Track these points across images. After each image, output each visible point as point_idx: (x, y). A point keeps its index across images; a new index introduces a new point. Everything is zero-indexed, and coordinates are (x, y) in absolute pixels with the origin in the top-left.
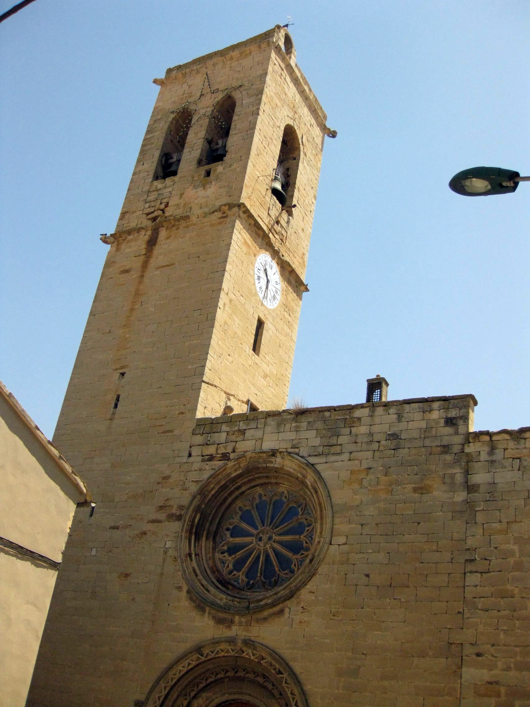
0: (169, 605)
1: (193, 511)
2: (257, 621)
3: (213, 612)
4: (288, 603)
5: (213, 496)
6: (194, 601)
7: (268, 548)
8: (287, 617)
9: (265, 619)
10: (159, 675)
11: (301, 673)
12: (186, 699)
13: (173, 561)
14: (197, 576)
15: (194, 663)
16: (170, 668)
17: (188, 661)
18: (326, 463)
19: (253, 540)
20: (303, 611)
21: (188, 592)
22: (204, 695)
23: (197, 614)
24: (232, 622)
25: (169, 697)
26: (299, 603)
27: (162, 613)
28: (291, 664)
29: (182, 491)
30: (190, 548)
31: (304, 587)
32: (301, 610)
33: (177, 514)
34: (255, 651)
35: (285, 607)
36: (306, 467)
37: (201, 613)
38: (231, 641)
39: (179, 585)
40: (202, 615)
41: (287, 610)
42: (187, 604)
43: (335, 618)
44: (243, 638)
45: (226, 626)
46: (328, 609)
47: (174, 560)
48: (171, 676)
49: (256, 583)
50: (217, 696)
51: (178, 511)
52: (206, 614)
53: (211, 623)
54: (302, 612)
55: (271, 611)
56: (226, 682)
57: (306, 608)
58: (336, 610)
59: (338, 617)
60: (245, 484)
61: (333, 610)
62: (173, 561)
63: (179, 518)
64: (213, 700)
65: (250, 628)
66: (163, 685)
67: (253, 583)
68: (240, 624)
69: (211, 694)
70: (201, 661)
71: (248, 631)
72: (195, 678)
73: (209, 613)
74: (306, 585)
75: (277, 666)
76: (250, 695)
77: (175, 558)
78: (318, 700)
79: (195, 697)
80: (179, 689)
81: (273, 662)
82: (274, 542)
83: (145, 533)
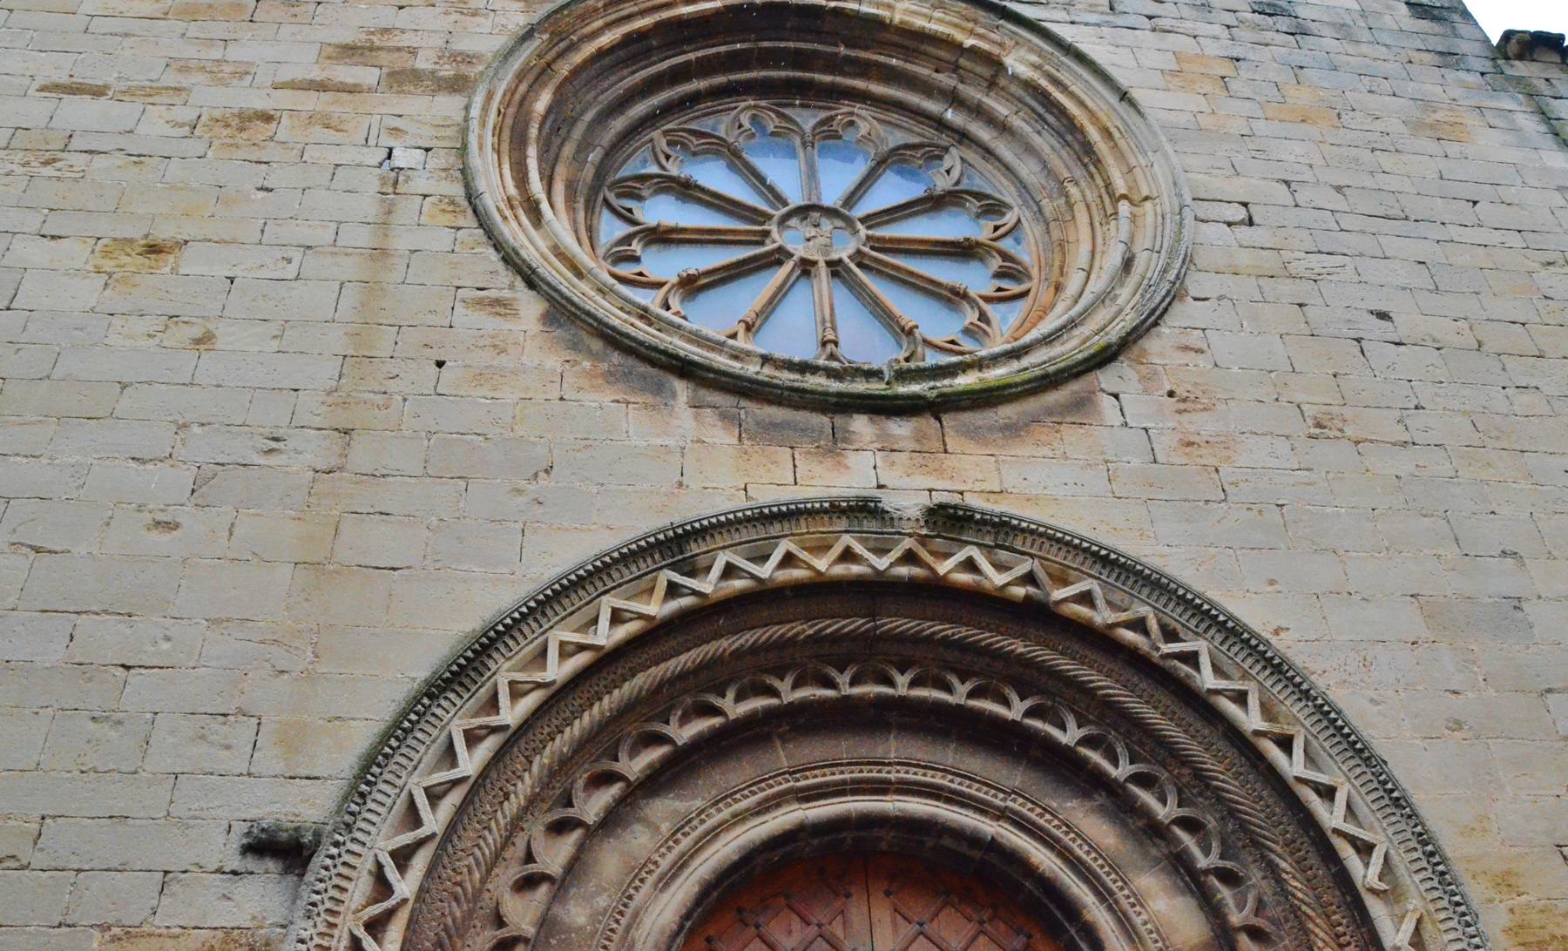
0: (440, 364)
1: (520, 77)
2: (973, 434)
5: (601, 54)
7: (847, 260)
9: (1012, 430)
12: (559, 828)
13: (444, 211)
14: (579, 274)
15: (657, 608)
17: (608, 603)
18: (1072, 23)
19: (767, 234)
20: (1182, 406)
29: (455, 17)
30: (522, 179)
31: (1148, 330)
33: (441, 73)
34: (1003, 555)
36: (1002, 22)
37: (650, 399)
38: (864, 510)
39: (493, 294)
40: (654, 407)
41: (1107, 402)
42: (553, 362)
44: (924, 500)
47: (451, 208)
51: (447, 66)
54: (1180, 412)
60: (705, 67)
62: (444, 211)
63: (458, 85)
65: (949, 461)
70: (686, 601)
71: (939, 472)
74: (1155, 324)
76: (933, 792)
77: (452, 203)
82: (864, 245)
83: (267, 118)
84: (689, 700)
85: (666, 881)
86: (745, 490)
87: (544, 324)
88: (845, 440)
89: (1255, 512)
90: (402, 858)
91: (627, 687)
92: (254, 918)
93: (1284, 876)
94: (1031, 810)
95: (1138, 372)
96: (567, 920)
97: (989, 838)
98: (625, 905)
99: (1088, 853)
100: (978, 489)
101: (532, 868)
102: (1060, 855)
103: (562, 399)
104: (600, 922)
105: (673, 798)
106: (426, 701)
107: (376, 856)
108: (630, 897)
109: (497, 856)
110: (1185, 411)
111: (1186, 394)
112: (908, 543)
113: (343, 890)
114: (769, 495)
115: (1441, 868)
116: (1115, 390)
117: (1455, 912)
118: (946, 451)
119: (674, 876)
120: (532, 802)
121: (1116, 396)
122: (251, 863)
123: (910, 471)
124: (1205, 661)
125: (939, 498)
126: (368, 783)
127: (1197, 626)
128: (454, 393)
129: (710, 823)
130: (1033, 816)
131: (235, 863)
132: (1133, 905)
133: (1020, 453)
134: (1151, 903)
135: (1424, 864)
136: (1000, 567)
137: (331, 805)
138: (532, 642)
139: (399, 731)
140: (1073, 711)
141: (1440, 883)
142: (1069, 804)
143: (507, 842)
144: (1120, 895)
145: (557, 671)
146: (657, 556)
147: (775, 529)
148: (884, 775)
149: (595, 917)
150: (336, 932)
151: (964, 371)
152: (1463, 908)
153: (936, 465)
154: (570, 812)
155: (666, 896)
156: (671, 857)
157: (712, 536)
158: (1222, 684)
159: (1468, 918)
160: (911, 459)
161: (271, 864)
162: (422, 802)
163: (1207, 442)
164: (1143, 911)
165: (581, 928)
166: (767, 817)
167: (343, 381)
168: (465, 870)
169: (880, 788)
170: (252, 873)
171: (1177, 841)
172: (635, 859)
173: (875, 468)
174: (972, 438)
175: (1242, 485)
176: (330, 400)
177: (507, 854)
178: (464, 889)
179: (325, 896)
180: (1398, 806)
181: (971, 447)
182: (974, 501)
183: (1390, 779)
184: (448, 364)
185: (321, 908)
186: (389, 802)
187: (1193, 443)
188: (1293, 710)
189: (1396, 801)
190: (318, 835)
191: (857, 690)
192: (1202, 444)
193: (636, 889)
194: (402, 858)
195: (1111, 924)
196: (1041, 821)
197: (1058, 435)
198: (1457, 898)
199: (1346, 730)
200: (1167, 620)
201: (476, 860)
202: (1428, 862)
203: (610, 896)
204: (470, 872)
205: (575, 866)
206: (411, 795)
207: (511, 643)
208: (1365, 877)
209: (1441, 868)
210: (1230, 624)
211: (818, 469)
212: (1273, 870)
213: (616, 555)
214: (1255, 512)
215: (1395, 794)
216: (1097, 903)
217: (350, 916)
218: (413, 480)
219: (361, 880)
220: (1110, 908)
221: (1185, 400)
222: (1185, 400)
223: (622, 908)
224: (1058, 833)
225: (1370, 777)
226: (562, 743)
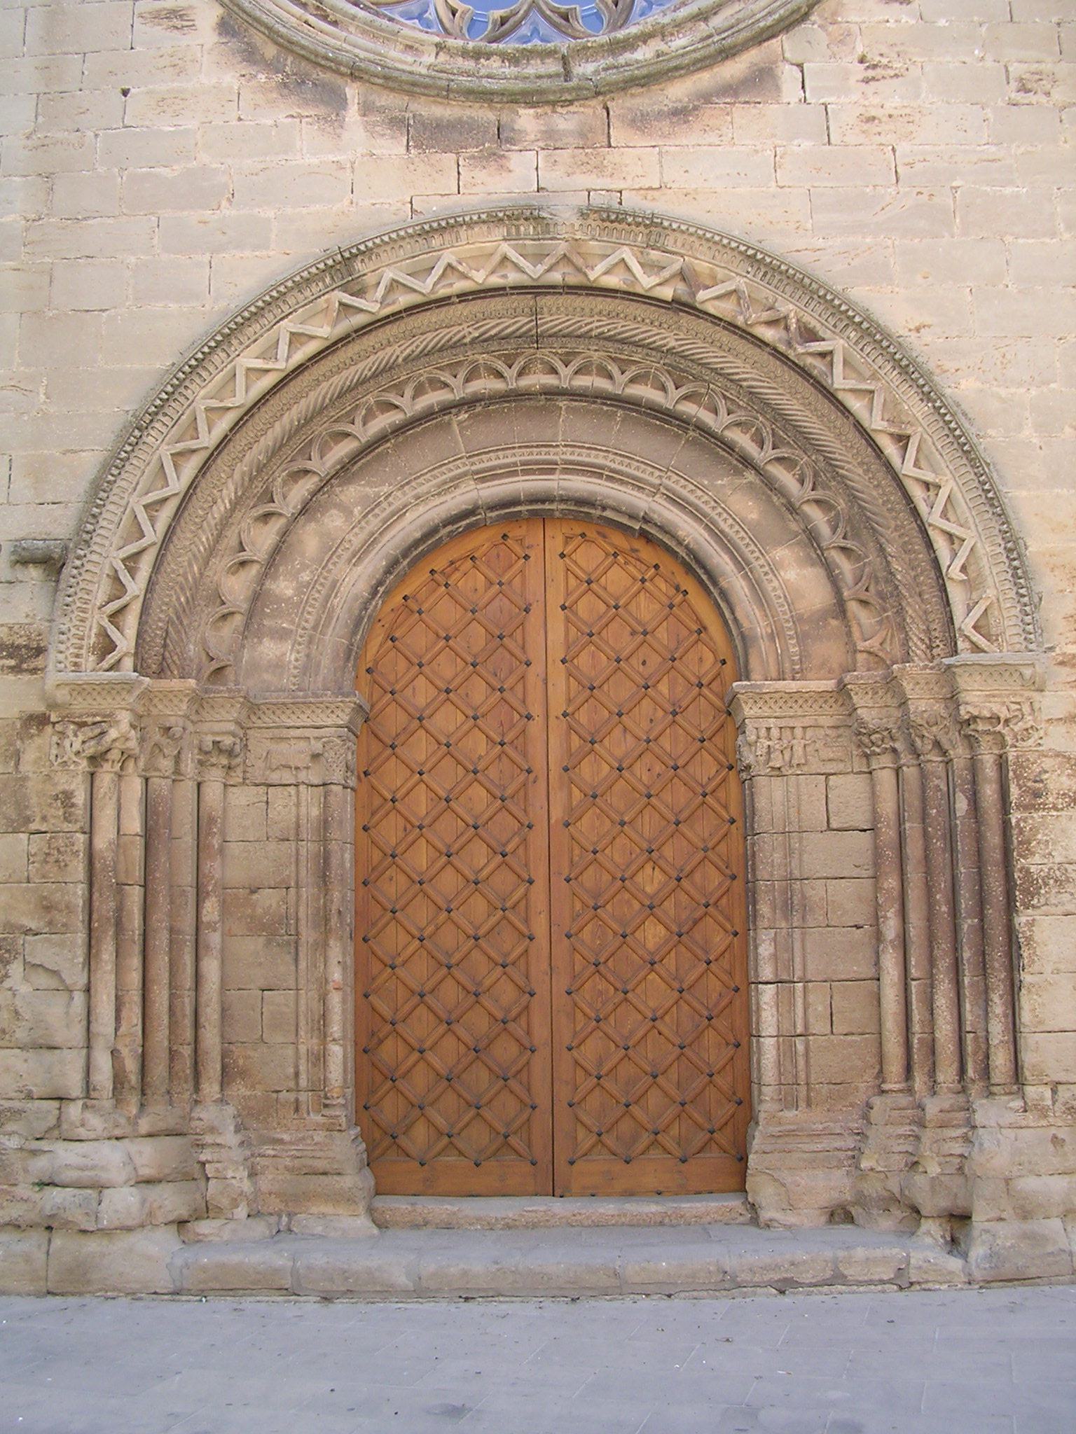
0: (125, 93)
2: (640, 122)
3: (386, 99)
4: (785, 44)
6: (272, 66)
8: (794, 100)
9: (681, 114)
10: (131, 407)
11: (918, 330)
15: (325, 331)
16: (195, 366)
17: (288, 326)
20: (871, 73)
21: (225, 27)
22: (351, 493)
23: (301, 117)
24: (503, 135)
25: (197, 507)
26: (844, 39)
27: (90, 134)
28: (862, 294)
32: (859, 71)
34: (655, 255)
35: (775, 62)
37: (322, 110)
41: (788, 75)
42: (230, 79)
43: (1031, 97)
44: (581, 199)
45: (473, 157)
46: (989, 63)
48: (200, 406)
49: (523, 18)
50: (420, 490)
52: (352, 113)
53: (393, 147)
54: (867, 81)
55: (704, 80)
56: (455, 427)
57: (884, 61)
58: (1034, 67)
59: (1048, 94)
61: (1016, 69)
64: (400, 513)
65: (612, 156)
66: (166, 452)
67: (504, 21)
68: (551, 141)
69: (386, 489)
71: (600, 168)
72: (309, 420)
73: (366, 109)
75: (787, 307)
76: (594, 471)
78: (1028, 433)
79: (306, 510)
80: (242, 468)
81: (766, 293)
84: (371, 399)
85: (359, 556)
86: (411, 203)
87: (220, 34)
88: (511, 141)
89: (925, 197)
90: (131, 562)
91: (313, 395)
92: (27, 616)
93: (889, 558)
94: (684, 487)
95: (829, 34)
96: (277, 592)
97: (642, 514)
98: (325, 578)
99: (731, 526)
100: (637, 187)
101: (243, 556)
102: (707, 527)
103: (240, 119)
104: (305, 594)
105: (363, 485)
106: (137, 433)
107: (111, 563)
108: (329, 571)
109: (212, 551)
110: (873, 79)
111: (878, 58)
112: (562, 248)
113: (89, 592)
114: (434, 207)
115: (1016, 563)
116: (799, 61)
117: (1019, 602)
118: (610, 146)
119: (366, 552)
120: (236, 504)
121: (800, 66)
122: (21, 573)
123: (570, 170)
124: (838, 359)
125: (598, 200)
126: (98, 506)
127: (835, 326)
128: (140, 123)
129: (397, 504)
130: (684, 493)
131: (6, 574)
132: (766, 574)
133: (685, 142)
134: (782, 573)
135: (1004, 559)
136: (648, 266)
137: (73, 523)
138: (222, 370)
139: (116, 463)
140: (725, 397)
141: (1012, 576)
142: (720, 482)
143: (219, 537)
144: (756, 564)
145: (242, 397)
146: (328, 280)
147: (436, 242)
148: (551, 457)
149: (299, 590)
150: (88, 624)
151: (645, 42)
152: (1026, 600)
153: (593, 162)
154: (270, 508)
155: (359, 569)
156: (363, 536)
157: (378, 255)
158: (852, 384)
159: (1027, 608)
160: (574, 157)
161: (34, 573)
162: (143, 517)
163: (890, 116)
164: (774, 578)
165: (289, 598)
166: (448, 497)
167: (40, 119)
168: (186, 564)
169: (548, 468)
170: (21, 582)
171: (806, 519)
172: (333, 540)
173: (537, 169)
174: (638, 129)
175: (918, 166)
176: (30, 143)
177: (221, 546)
178: (186, 579)
179: (76, 598)
180: (992, 505)
181: (638, 140)
182: (632, 202)
183: (990, 480)
184: (132, 91)
185: (74, 607)
186: (116, 519)
187: (874, 118)
188: (916, 409)
189: (992, 500)
190: (66, 548)
191: (525, 382)
192: (884, 119)
193: (334, 564)
194: (131, 562)
195: (746, 590)
196: (692, 498)
197: (729, 118)
198: (1022, 591)
199: (958, 432)
200: (806, 318)
201: (194, 556)
202: (1008, 557)
203: (312, 572)
204: (190, 565)
205: (278, 552)
206: (133, 510)
207: (204, 374)
208: (949, 566)
209: (1016, 563)
210: (865, 325)
211: (481, 175)
212: (882, 549)
213: (290, 284)
214: (925, 197)
215: (990, 495)
216: (735, 570)
217: (96, 611)
218: (111, 221)
219: (103, 582)
220: (746, 576)
221: (875, 67)
222: (875, 67)
223: (322, 580)
224: (707, 509)
225: (973, 476)
226: (257, 453)
